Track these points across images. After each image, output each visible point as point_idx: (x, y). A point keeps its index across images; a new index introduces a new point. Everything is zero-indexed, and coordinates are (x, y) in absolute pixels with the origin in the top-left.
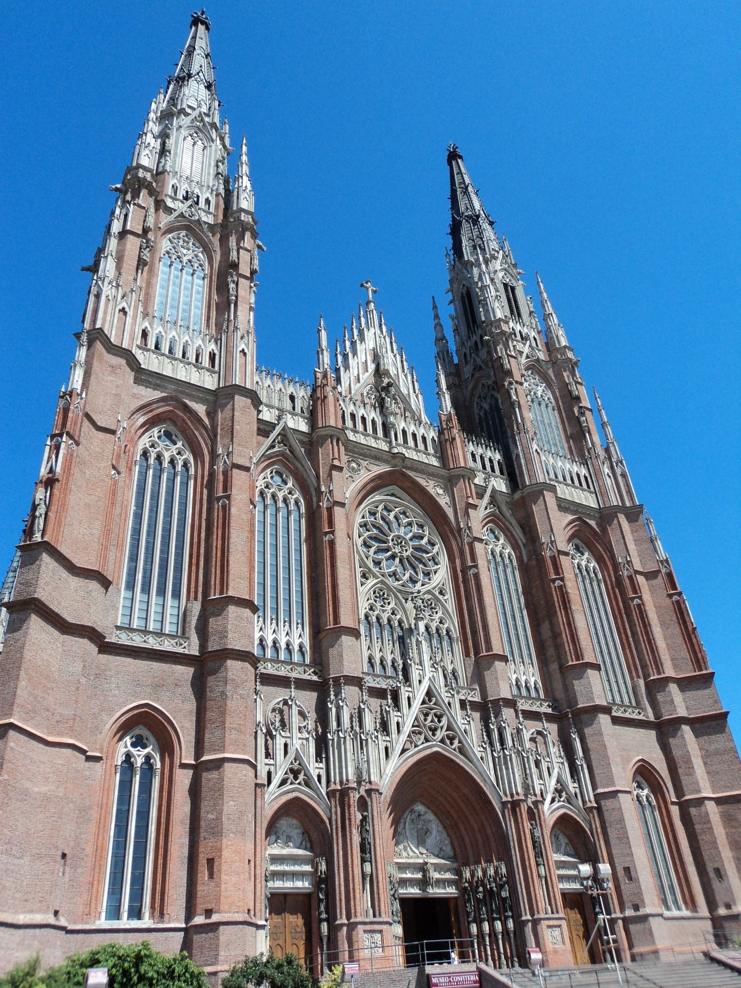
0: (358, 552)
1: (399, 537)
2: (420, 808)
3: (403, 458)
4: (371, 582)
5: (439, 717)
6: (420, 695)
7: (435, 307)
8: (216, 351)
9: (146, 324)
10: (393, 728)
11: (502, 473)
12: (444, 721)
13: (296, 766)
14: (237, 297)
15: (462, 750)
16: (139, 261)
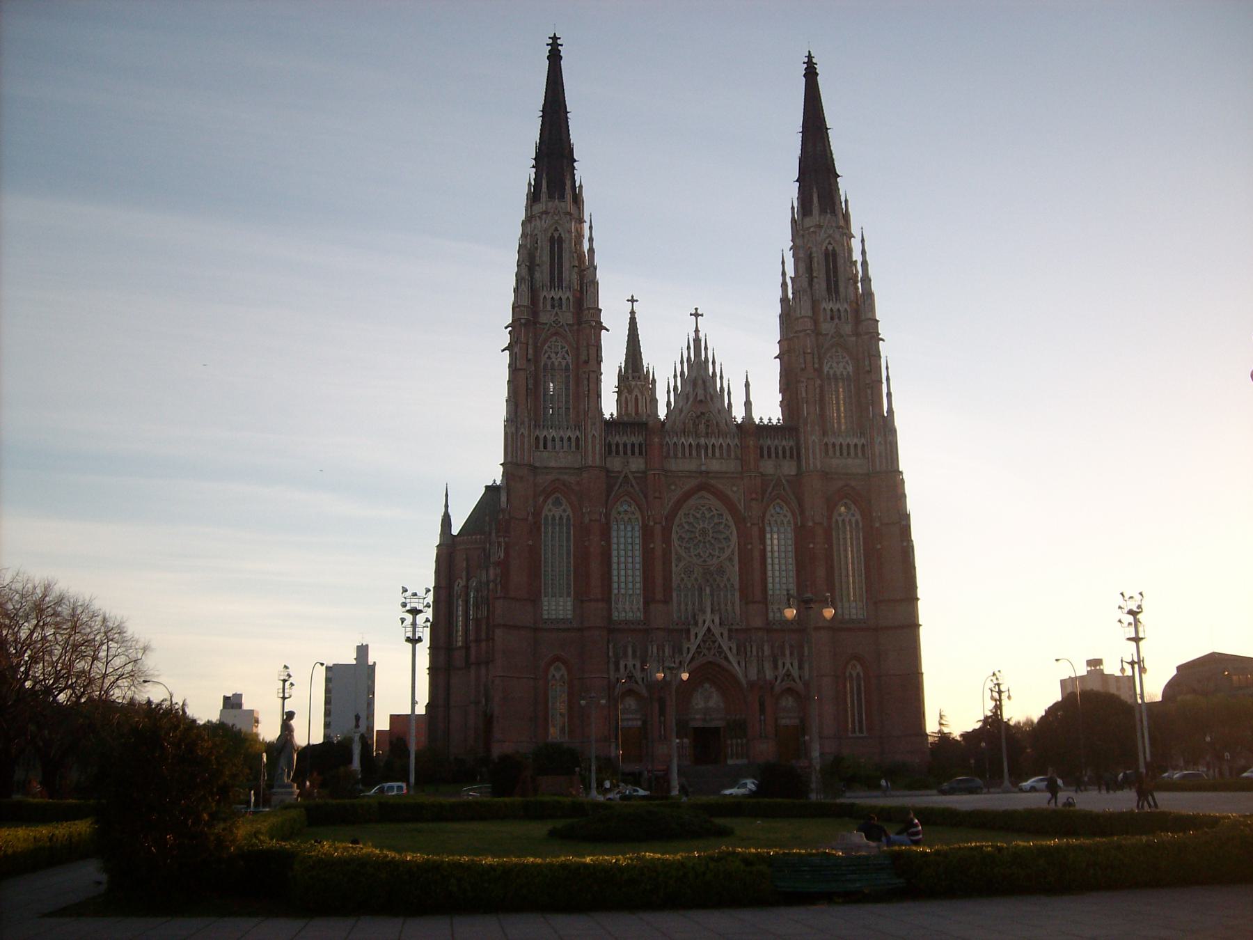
0: (674, 545)
1: (705, 528)
2: (707, 685)
3: (708, 473)
4: (681, 565)
5: (714, 642)
6: (702, 632)
7: (783, 263)
8: (579, 436)
9: (537, 432)
10: (685, 650)
11: (791, 457)
12: (716, 644)
13: (630, 675)
14: (589, 390)
15: (726, 658)
16: (527, 389)
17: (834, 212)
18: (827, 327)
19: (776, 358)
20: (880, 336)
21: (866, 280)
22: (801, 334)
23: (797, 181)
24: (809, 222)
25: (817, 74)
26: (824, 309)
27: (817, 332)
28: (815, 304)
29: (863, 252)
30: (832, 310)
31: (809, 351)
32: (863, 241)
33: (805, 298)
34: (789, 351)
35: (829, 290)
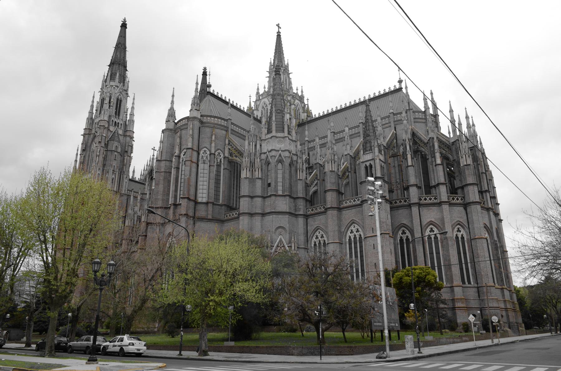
7: (94, 97)
17: (124, 83)
18: (112, 128)
19: (82, 135)
20: (133, 139)
21: (132, 115)
22: (102, 127)
23: (109, 66)
24: (112, 83)
25: (127, 28)
26: (113, 121)
27: (109, 130)
28: (110, 116)
29: (133, 103)
30: (115, 122)
31: (105, 135)
32: (134, 99)
33: (107, 113)
34: (89, 134)
35: (116, 114)
